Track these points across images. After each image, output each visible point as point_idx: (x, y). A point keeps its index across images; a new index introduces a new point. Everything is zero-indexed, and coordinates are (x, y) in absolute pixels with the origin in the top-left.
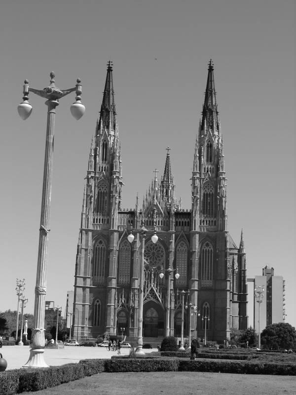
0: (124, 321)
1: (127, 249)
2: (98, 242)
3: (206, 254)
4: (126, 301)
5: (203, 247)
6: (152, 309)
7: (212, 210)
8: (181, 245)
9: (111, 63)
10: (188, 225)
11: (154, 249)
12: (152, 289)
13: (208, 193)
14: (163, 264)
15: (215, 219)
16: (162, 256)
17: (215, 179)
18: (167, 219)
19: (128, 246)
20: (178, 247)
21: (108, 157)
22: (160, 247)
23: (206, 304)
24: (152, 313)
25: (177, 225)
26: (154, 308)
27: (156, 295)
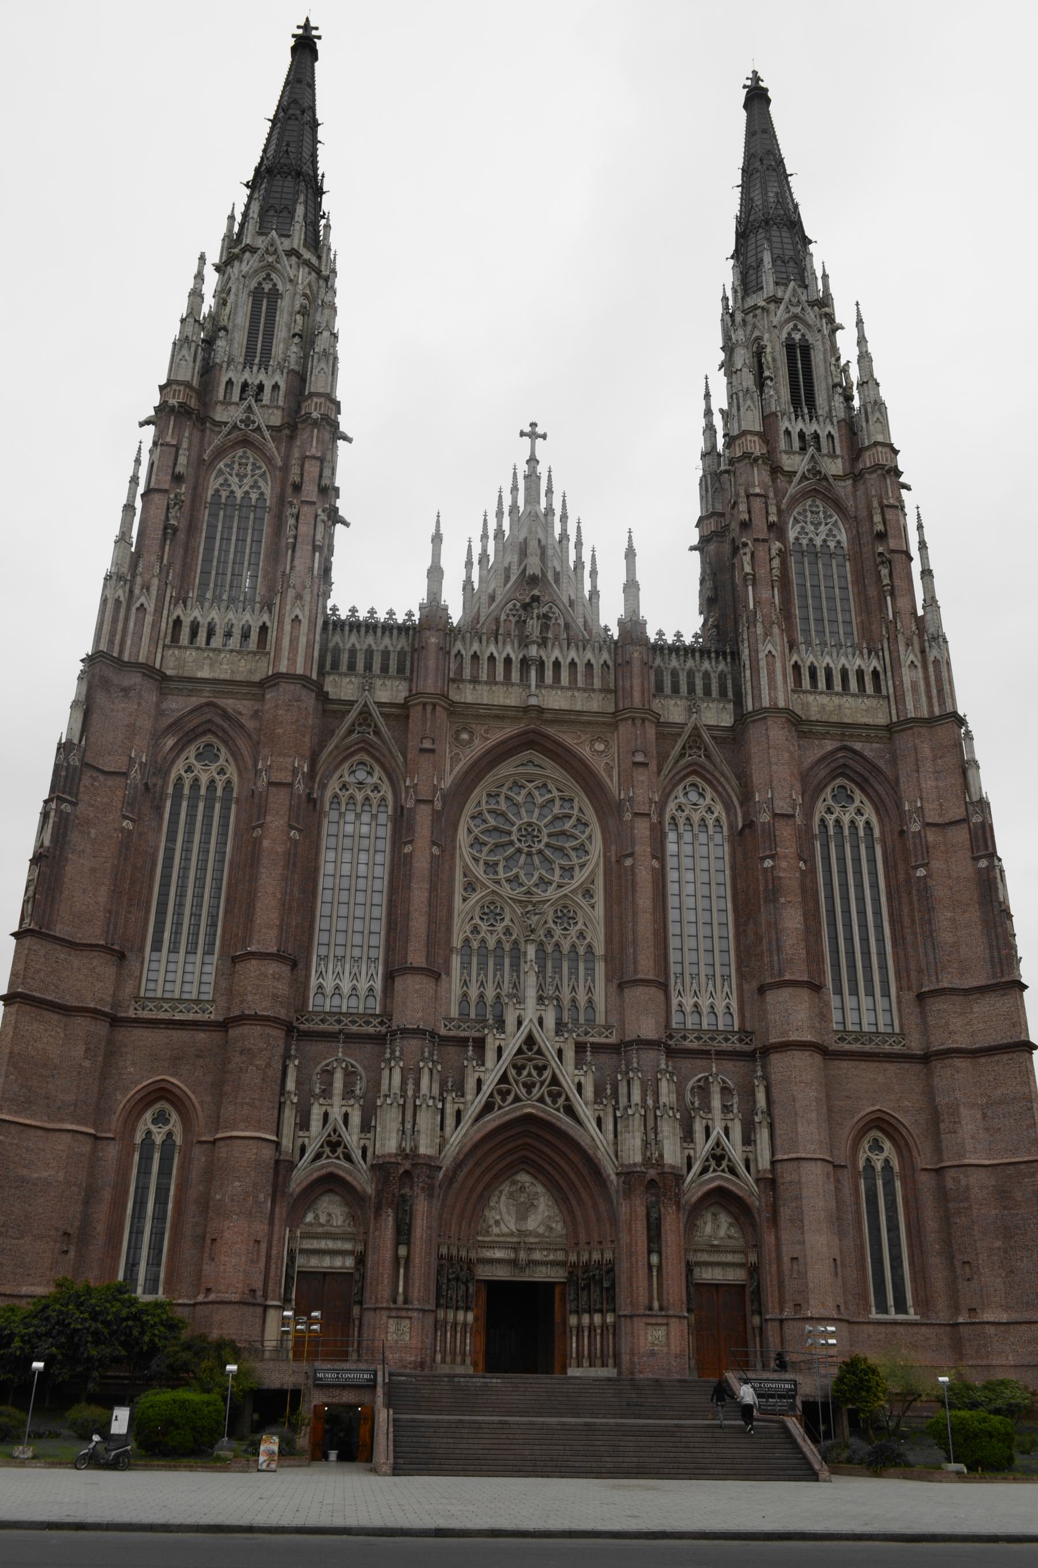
0: (338, 1262)
1: (367, 799)
3: (841, 847)
4: (356, 1119)
5: (820, 808)
6: (524, 1178)
7: (848, 623)
8: (686, 794)
10: (723, 693)
11: (530, 812)
12: (530, 1040)
13: (818, 542)
14: (588, 894)
15: (875, 663)
16: (582, 849)
18: (605, 656)
19: (376, 788)
20: (671, 807)
21: (278, 349)
23: (877, 1147)
24: (523, 1212)
26: (539, 1172)
27: (555, 1081)
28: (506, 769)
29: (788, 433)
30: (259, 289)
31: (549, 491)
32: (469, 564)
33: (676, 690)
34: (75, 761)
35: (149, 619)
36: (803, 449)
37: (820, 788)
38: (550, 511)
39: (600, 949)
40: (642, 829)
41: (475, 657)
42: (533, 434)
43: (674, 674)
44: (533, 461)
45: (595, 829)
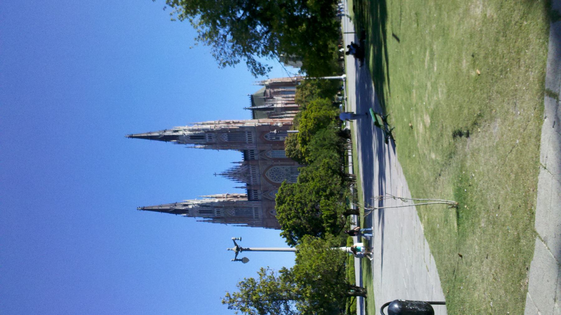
2: (272, 214)
9: (139, 209)
14: (283, 168)
17: (216, 133)
21: (209, 210)
22: (272, 170)
25: (253, 159)
28: (268, 177)
29: (209, 141)
30: (200, 213)
31: (225, 172)
32: (238, 182)
33: (253, 157)
34: (277, 228)
35: (256, 222)
36: (211, 139)
37: (266, 140)
38: (228, 172)
39: (290, 166)
40: (275, 163)
41: (253, 182)
42: (215, 175)
43: (251, 157)
44: (220, 175)
45: (275, 167)
